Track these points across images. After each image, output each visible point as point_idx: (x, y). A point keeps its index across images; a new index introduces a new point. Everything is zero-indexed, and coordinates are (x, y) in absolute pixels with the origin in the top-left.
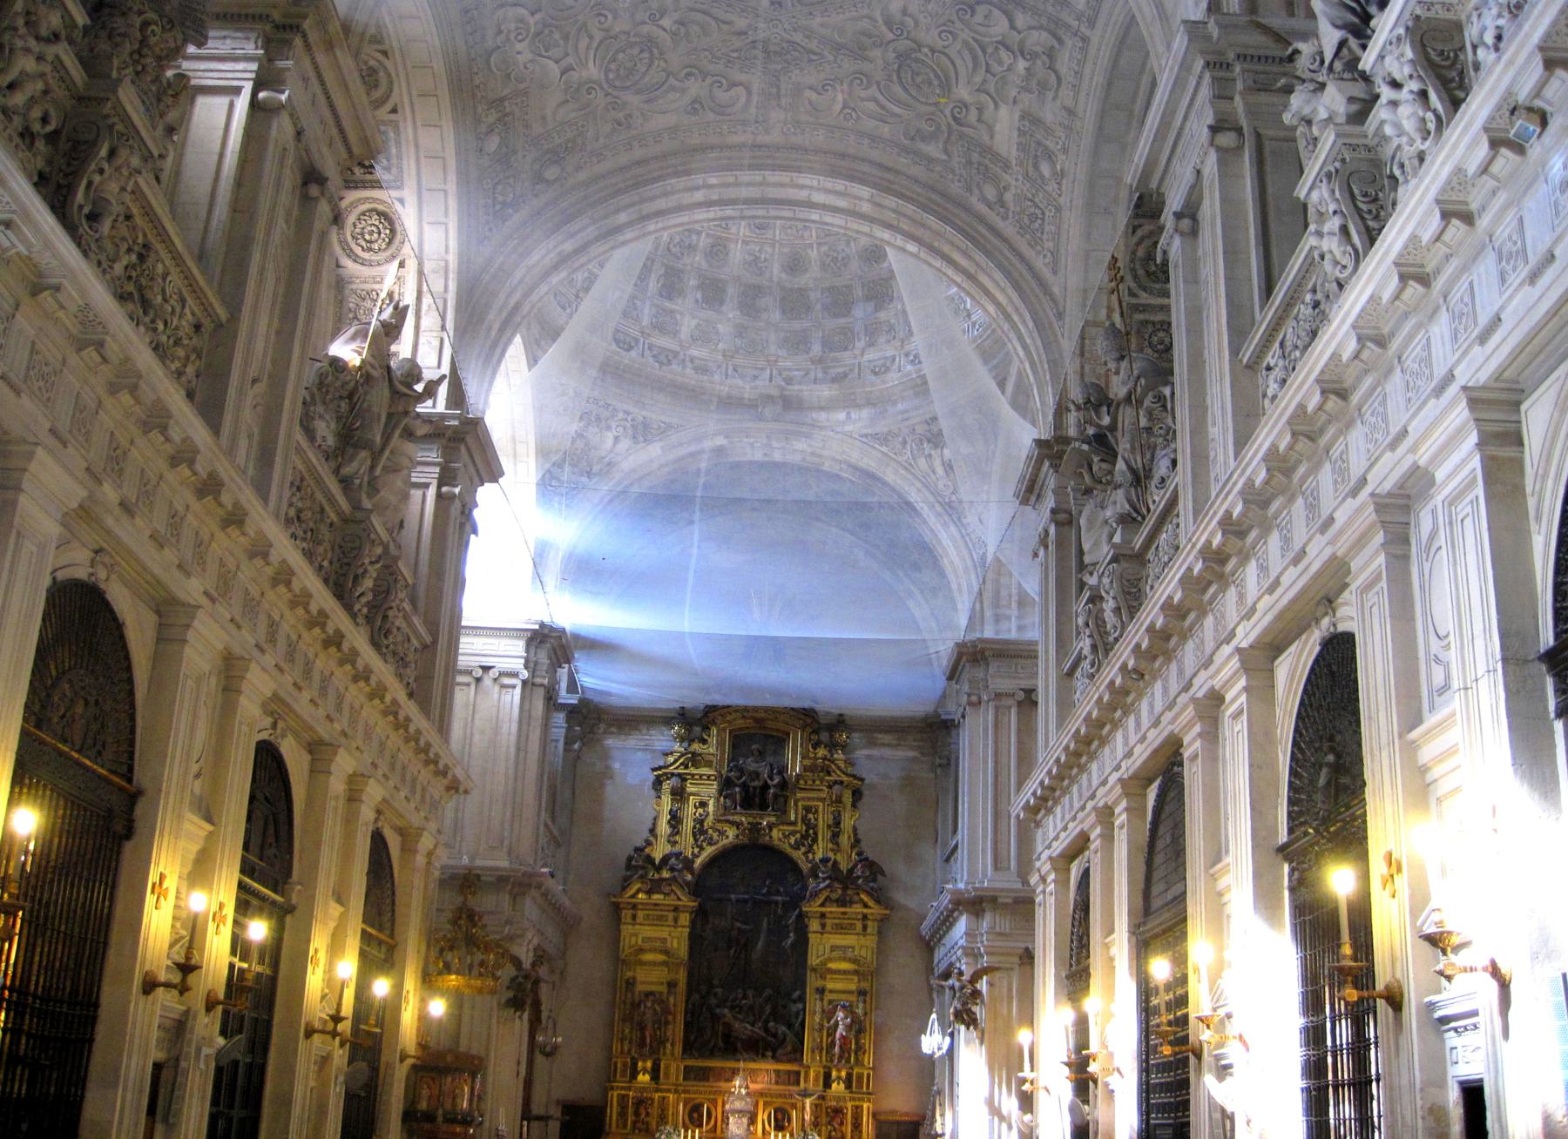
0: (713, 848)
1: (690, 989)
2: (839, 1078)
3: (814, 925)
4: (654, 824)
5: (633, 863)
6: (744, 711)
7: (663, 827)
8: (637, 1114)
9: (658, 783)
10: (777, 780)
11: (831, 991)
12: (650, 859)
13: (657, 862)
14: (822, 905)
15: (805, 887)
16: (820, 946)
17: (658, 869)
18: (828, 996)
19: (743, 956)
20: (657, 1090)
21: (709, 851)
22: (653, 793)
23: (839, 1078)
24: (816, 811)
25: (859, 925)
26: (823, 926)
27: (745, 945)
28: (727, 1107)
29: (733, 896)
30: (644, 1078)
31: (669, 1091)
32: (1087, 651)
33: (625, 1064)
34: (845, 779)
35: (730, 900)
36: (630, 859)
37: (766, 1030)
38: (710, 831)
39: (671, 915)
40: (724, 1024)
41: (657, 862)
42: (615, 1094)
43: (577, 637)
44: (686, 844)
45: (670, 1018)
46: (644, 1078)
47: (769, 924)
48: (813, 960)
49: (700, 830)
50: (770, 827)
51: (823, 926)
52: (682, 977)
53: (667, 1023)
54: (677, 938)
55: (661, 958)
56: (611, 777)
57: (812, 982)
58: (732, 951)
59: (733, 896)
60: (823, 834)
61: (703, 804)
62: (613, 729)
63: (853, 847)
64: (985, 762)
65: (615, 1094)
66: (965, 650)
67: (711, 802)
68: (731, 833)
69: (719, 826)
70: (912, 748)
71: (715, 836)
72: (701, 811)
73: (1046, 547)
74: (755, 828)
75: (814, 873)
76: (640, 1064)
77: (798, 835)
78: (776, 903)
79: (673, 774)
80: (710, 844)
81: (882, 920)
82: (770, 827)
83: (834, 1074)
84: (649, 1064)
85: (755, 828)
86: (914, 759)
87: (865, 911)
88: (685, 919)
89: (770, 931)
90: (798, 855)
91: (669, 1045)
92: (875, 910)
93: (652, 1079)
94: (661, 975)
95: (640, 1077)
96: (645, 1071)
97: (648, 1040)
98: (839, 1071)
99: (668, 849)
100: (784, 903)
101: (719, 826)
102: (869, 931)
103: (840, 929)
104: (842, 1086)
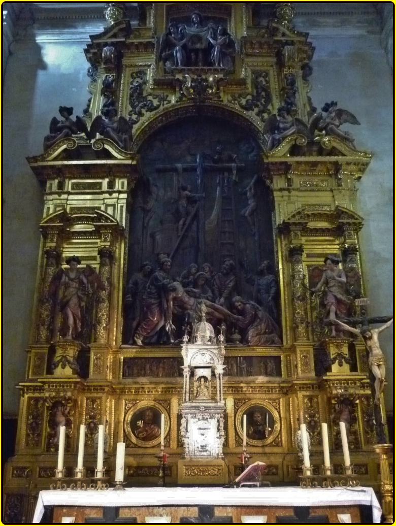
2: (340, 356)
3: (278, 183)
4: (89, 106)
10: (220, 39)
20: (85, 389)
21: (148, 116)
23: (340, 356)
24: (267, 75)
29: (179, 165)
30: (65, 372)
31: (100, 388)
35: (175, 170)
36: (54, 121)
37: (231, 307)
39: (105, 182)
45: (104, 294)
46: (65, 372)
47: (222, 191)
49: (137, 94)
52: (121, 251)
55: (89, 228)
58: (181, 222)
59: (179, 165)
74: (200, 87)
76: (59, 352)
77: (249, 97)
78: (229, 170)
83: (333, 351)
86: (361, 37)
89: (225, 199)
93: (75, 372)
95: (59, 371)
96: (65, 362)
98: (338, 346)
100: (239, 170)
104: (346, 367)
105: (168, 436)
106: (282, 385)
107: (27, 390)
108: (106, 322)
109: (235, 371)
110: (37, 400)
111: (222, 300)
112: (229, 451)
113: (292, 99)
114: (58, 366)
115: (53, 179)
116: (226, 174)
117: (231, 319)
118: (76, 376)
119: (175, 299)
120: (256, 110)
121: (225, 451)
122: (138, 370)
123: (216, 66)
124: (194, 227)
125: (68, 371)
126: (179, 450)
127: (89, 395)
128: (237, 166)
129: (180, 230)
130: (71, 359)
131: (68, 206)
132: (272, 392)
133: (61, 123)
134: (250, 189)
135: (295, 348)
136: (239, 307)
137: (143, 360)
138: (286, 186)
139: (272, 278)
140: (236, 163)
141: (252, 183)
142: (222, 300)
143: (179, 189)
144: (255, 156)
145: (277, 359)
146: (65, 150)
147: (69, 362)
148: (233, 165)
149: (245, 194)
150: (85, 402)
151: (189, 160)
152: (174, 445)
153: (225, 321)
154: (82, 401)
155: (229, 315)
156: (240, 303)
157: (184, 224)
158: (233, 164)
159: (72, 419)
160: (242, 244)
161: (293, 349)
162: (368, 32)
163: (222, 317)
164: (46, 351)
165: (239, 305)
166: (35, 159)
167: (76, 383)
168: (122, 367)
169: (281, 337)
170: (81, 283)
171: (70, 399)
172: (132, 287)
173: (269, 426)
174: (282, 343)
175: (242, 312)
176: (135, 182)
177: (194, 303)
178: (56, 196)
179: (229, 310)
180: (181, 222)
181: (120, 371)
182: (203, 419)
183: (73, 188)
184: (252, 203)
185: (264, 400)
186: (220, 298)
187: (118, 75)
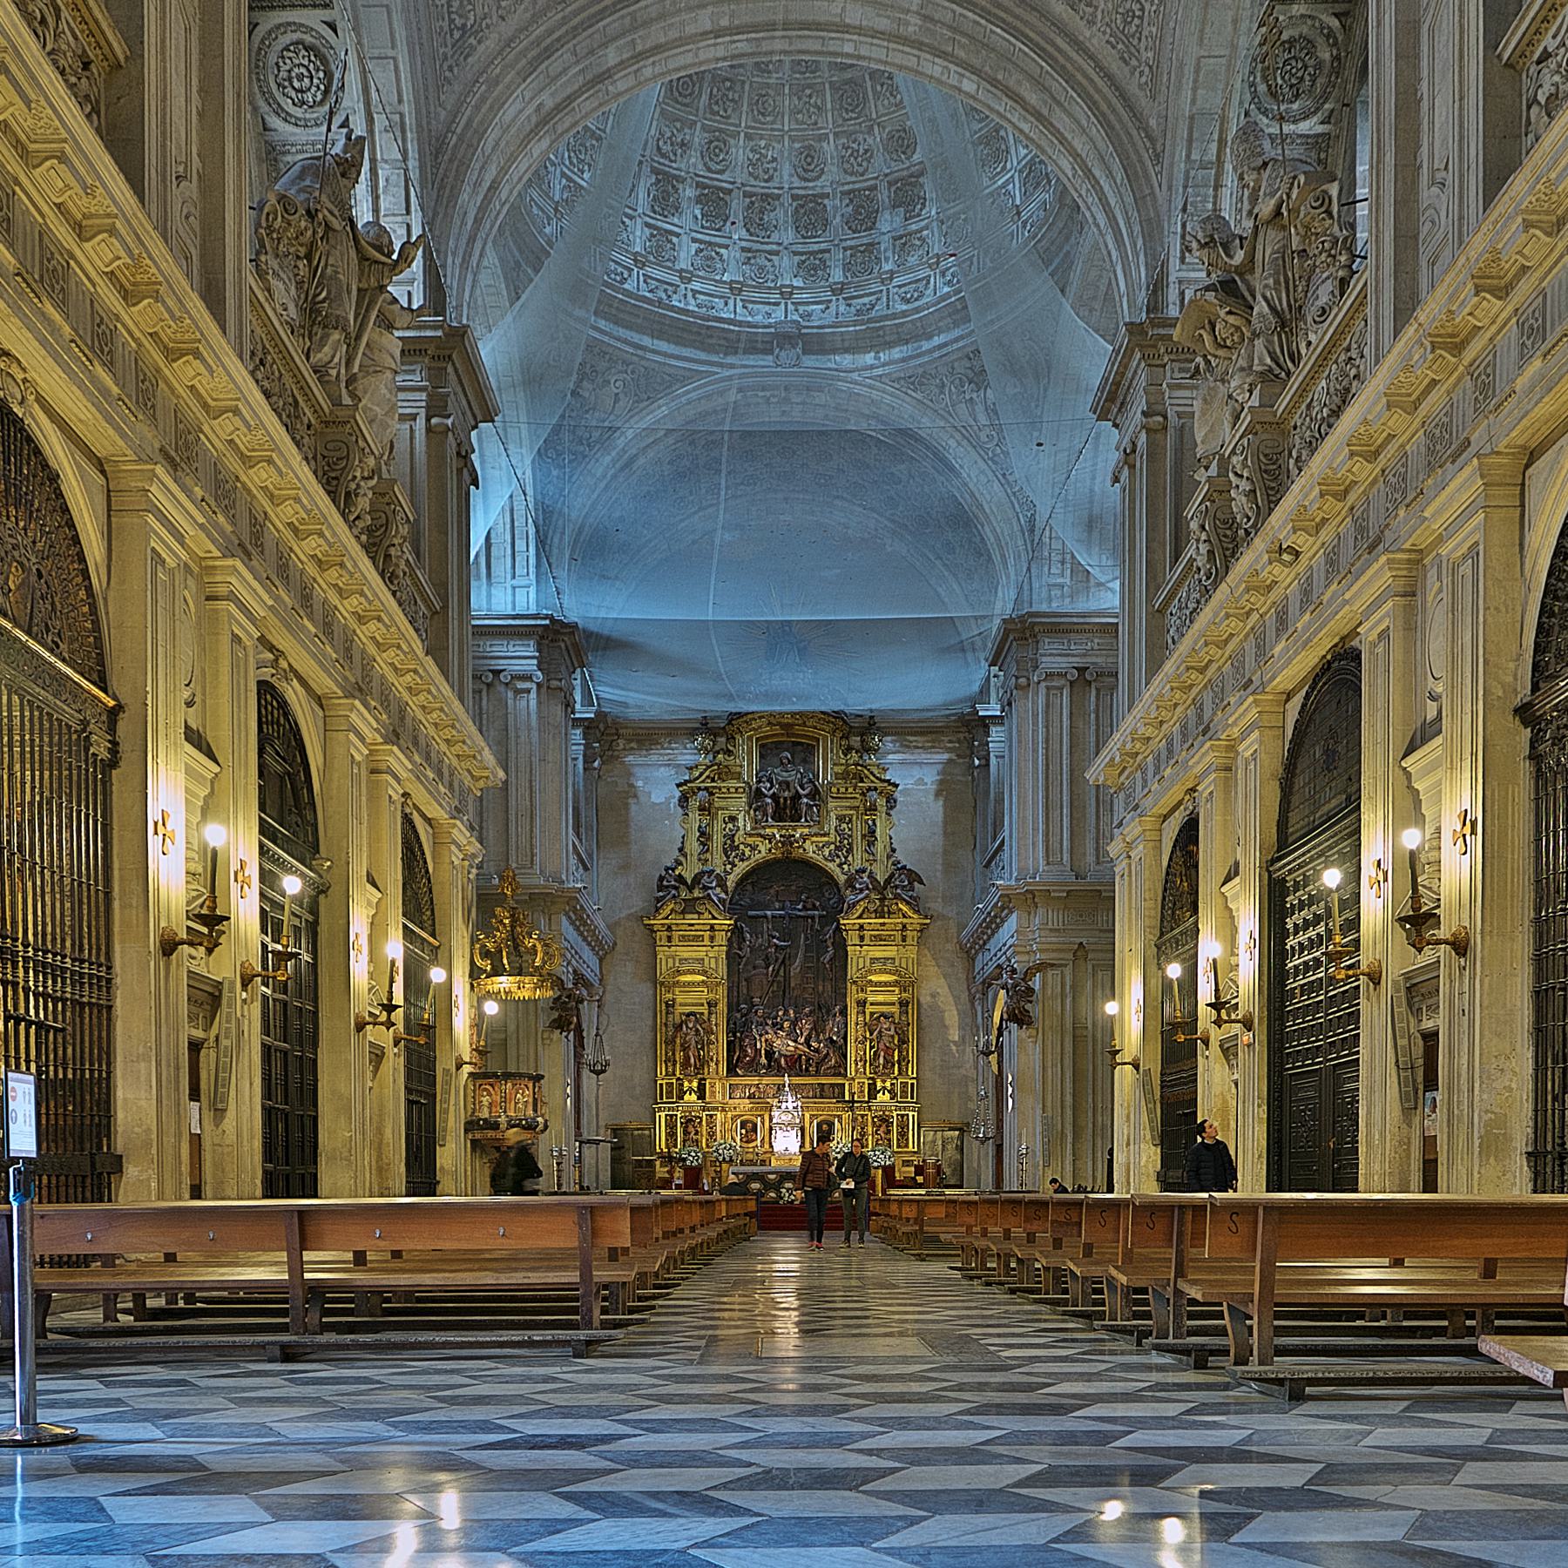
0: (746, 863)
1: (732, 1007)
3: (852, 938)
5: (665, 883)
6: (772, 718)
7: (693, 846)
8: (686, 1133)
9: (684, 800)
11: (872, 1004)
12: (680, 879)
13: (689, 882)
14: (860, 917)
15: (842, 900)
16: (859, 956)
17: (691, 889)
18: (869, 1009)
19: (782, 973)
21: (742, 867)
24: (850, 821)
25: (898, 935)
26: (862, 938)
27: (783, 962)
29: (769, 913)
30: (691, 1098)
31: (716, 1109)
32: (1201, 561)
34: (879, 784)
35: (766, 917)
36: (661, 879)
37: (809, 1046)
38: (742, 847)
40: (766, 1040)
41: (689, 882)
42: (663, 1114)
43: (589, 635)
44: (717, 862)
47: (806, 939)
48: (852, 972)
49: (730, 847)
50: (804, 838)
51: (862, 938)
52: (721, 994)
53: (710, 1043)
54: (714, 955)
56: (635, 796)
57: (853, 995)
60: (859, 845)
61: (733, 819)
62: (633, 745)
63: (889, 857)
64: (1035, 751)
65: (663, 1114)
66: (1013, 626)
67: (740, 817)
68: (763, 847)
69: (750, 840)
70: (949, 750)
71: (747, 853)
72: (730, 825)
73: (1132, 467)
74: (788, 841)
75: (850, 883)
76: (686, 1084)
77: (832, 847)
79: (699, 789)
80: (742, 860)
81: (921, 931)
82: (804, 838)
83: (879, 1084)
85: (788, 841)
86: (950, 761)
87: (905, 921)
88: (721, 938)
89: (808, 948)
90: (832, 867)
91: (713, 1064)
92: (915, 920)
94: (704, 995)
95: (686, 1097)
96: (691, 1090)
97: (692, 1060)
99: (697, 868)
101: (750, 840)
102: (909, 941)
103: (878, 939)
110: (671, 1116)
119: (766, 1040)
120: (838, 861)
124: (782, 973)
125: (694, 1097)
152: (767, 1146)
170: (697, 1030)
175: (817, 1051)
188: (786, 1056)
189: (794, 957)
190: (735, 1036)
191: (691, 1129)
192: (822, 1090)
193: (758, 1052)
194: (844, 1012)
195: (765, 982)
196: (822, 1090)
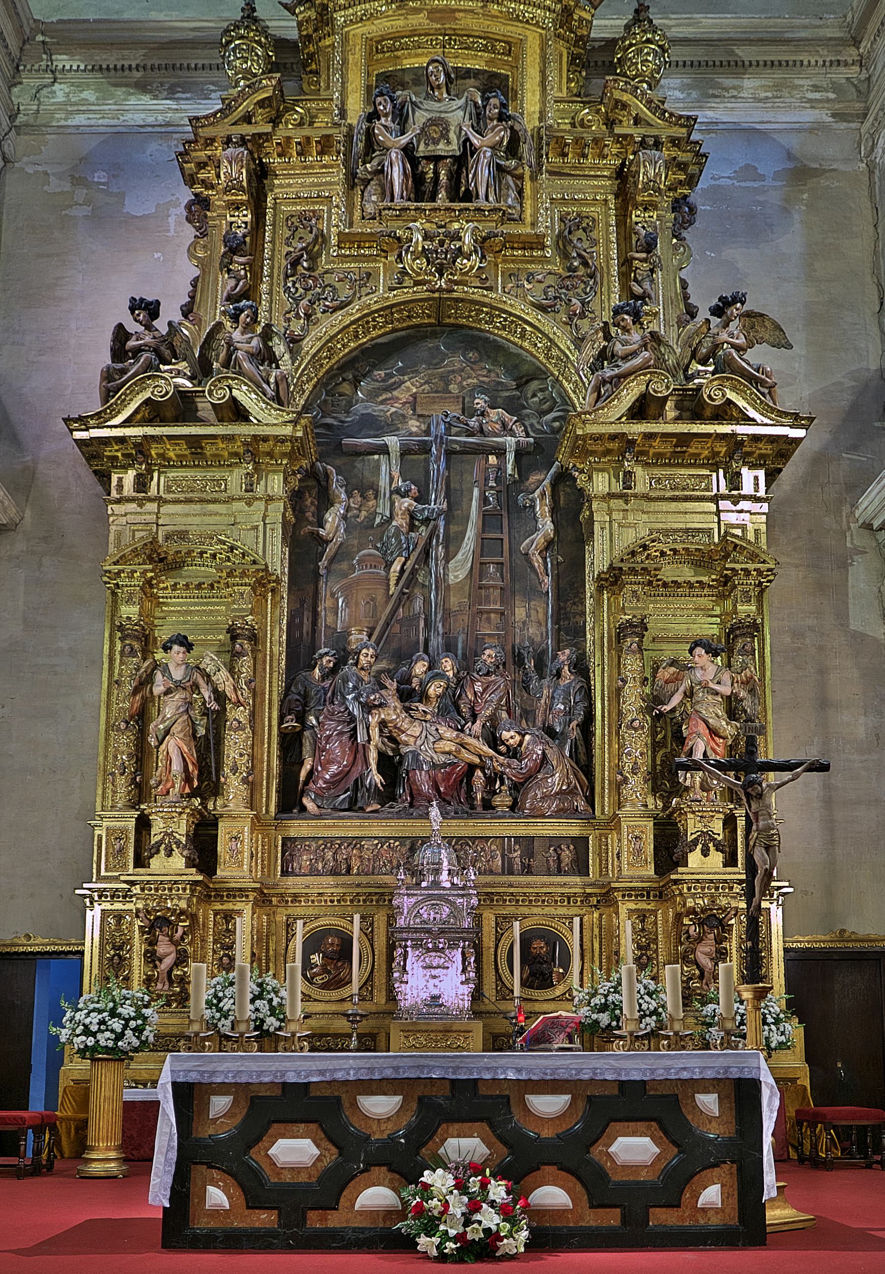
22: (189, 232)
28: (401, 922)
33: (117, 835)
35: (384, 450)
37: (494, 741)
40: (383, 724)
47: (484, 500)
58: (396, 567)
78: (500, 452)
84: (182, 828)
89: (488, 520)
93: (190, 863)
95: (156, 863)
102: (747, 488)
105: (368, 982)
106: (588, 891)
107: (100, 897)
108: (247, 768)
109: (500, 863)
111: (477, 727)
112: (483, 1008)
113: (647, 285)
114: (158, 852)
115: (125, 468)
116: (492, 459)
117: (495, 764)
118: (194, 870)
119: (383, 724)
121: (476, 1008)
122: (311, 860)
123: (482, 203)
125: (178, 862)
126: (390, 1006)
127: (218, 907)
128: (518, 443)
129: (392, 582)
130: (183, 840)
131: (160, 528)
132: (569, 903)
133: (134, 338)
134: (543, 494)
135: (619, 821)
136: (511, 741)
137: (321, 842)
138: (618, 488)
139: (580, 684)
140: (513, 435)
141: (547, 482)
142: (477, 727)
143: (391, 493)
144: (555, 419)
145: (581, 843)
146: (148, 402)
147: (178, 843)
148: (510, 441)
149: (533, 507)
150: (212, 919)
151: (414, 429)
152: (380, 998)
153: (483, 769)
154: (206, 918)
155: (491, 758)
156: (512, 733)
157: (402, 571)
158: (509, 438)
159: (190, 950)
160: (520, 613)
161: (614, 823)
162: (833, 115)
163: (477, 760)
164: (132, 824)
165: (512, 738)
166: (83, 422)
167: (196, 883)
168: (279, 855)
169: (591, 802)
171: (182, 912)
172: (297, 700)
173: (560, 966)
174: (594, 813)
175: (514, 753)
176: (299, 476)
177: (422, 732)
178: (132, 507)
179: (490, 747)
180: (396, 567)
181: (277, 860)
182: (436, 949)
183: (168, 490)
184: (547, 526)
185: (554, 918)
186: (473, 723)
187: (257, 222)
188: (434, 766)
189: (452, 544)
190: (301, 718)
191: (163, 947)
192: (529, 853)
193: (358, 752)
194: (581, 668)
195: (380, 597)
196: (529, 853)
